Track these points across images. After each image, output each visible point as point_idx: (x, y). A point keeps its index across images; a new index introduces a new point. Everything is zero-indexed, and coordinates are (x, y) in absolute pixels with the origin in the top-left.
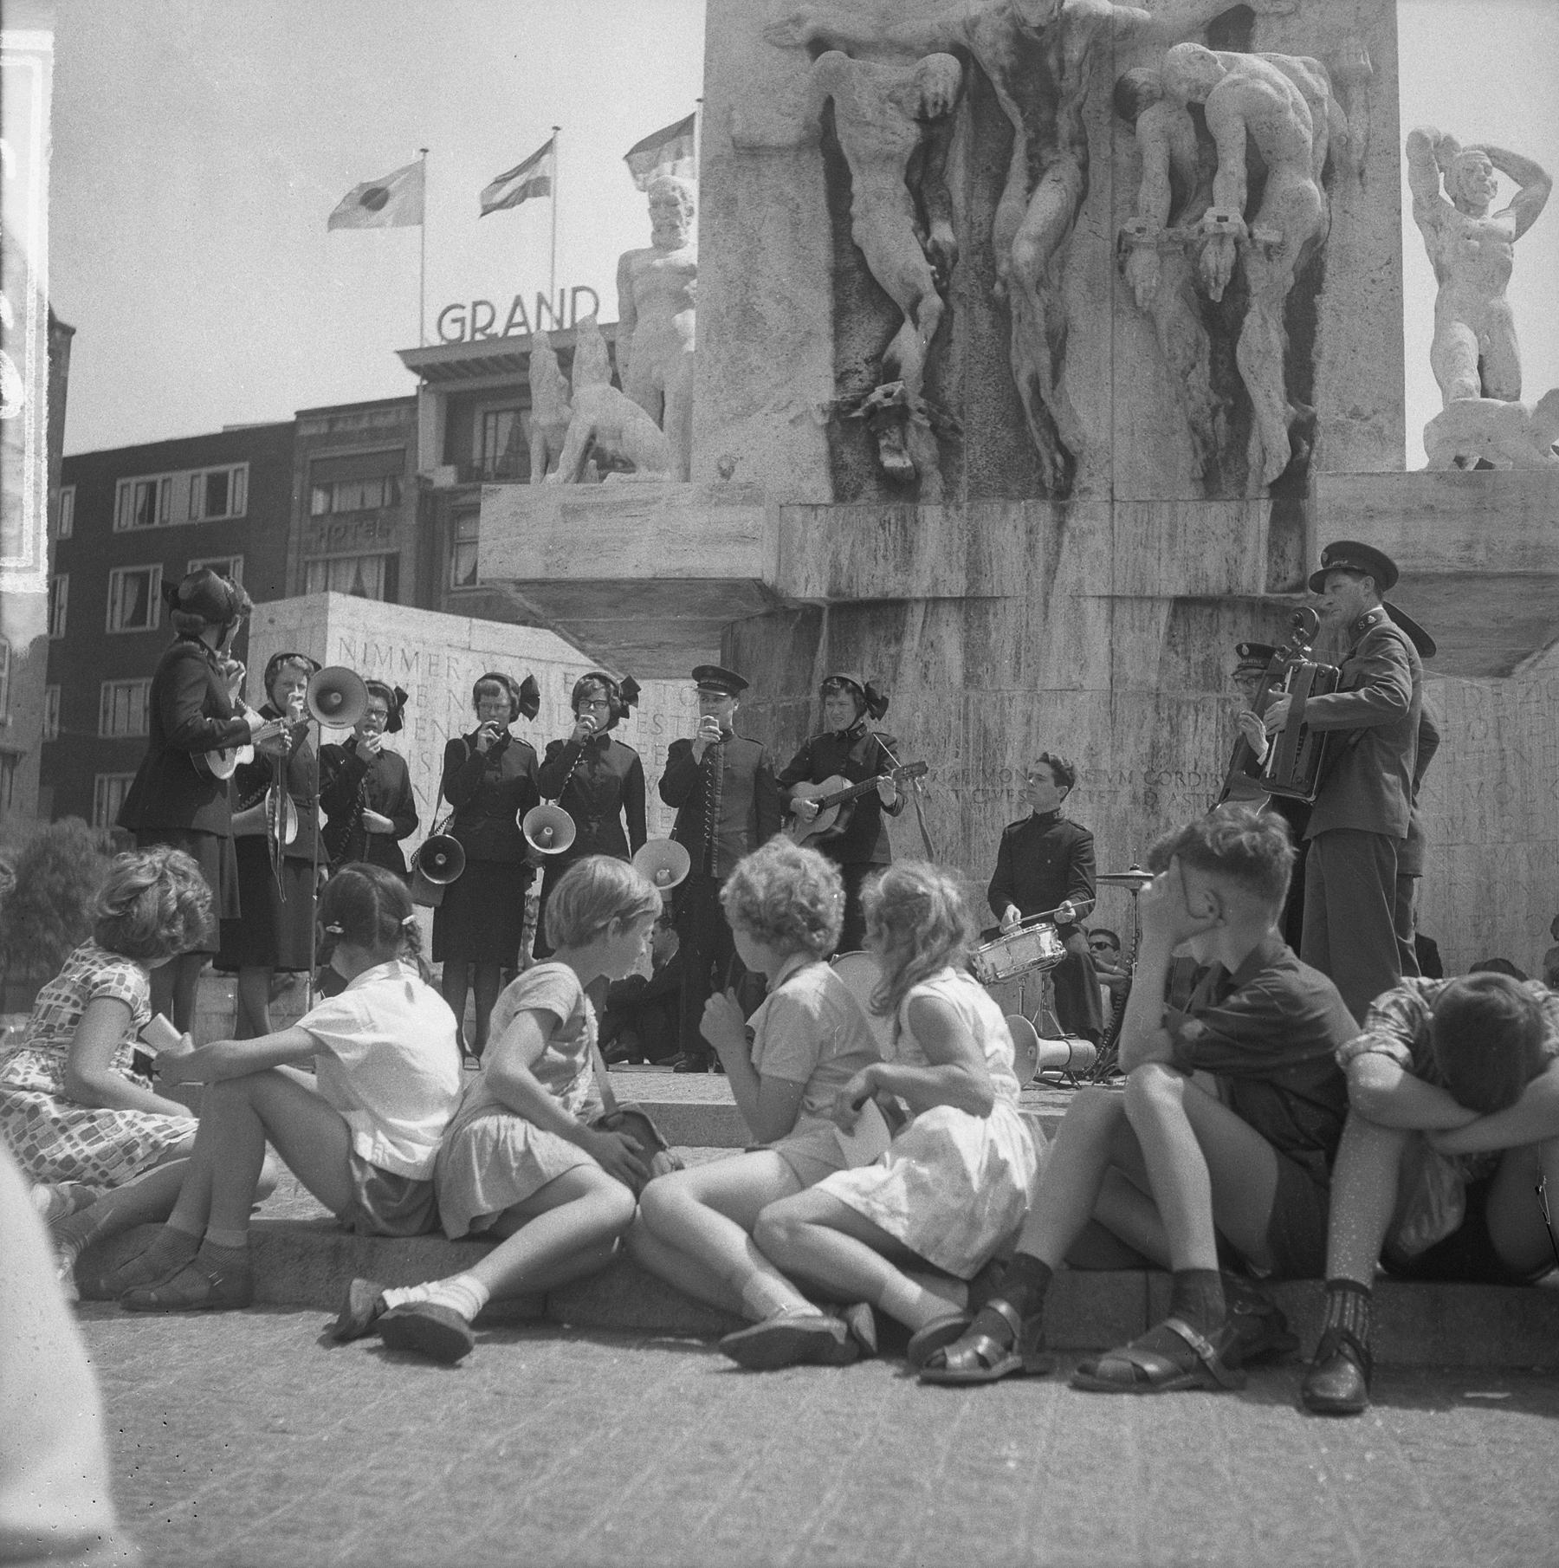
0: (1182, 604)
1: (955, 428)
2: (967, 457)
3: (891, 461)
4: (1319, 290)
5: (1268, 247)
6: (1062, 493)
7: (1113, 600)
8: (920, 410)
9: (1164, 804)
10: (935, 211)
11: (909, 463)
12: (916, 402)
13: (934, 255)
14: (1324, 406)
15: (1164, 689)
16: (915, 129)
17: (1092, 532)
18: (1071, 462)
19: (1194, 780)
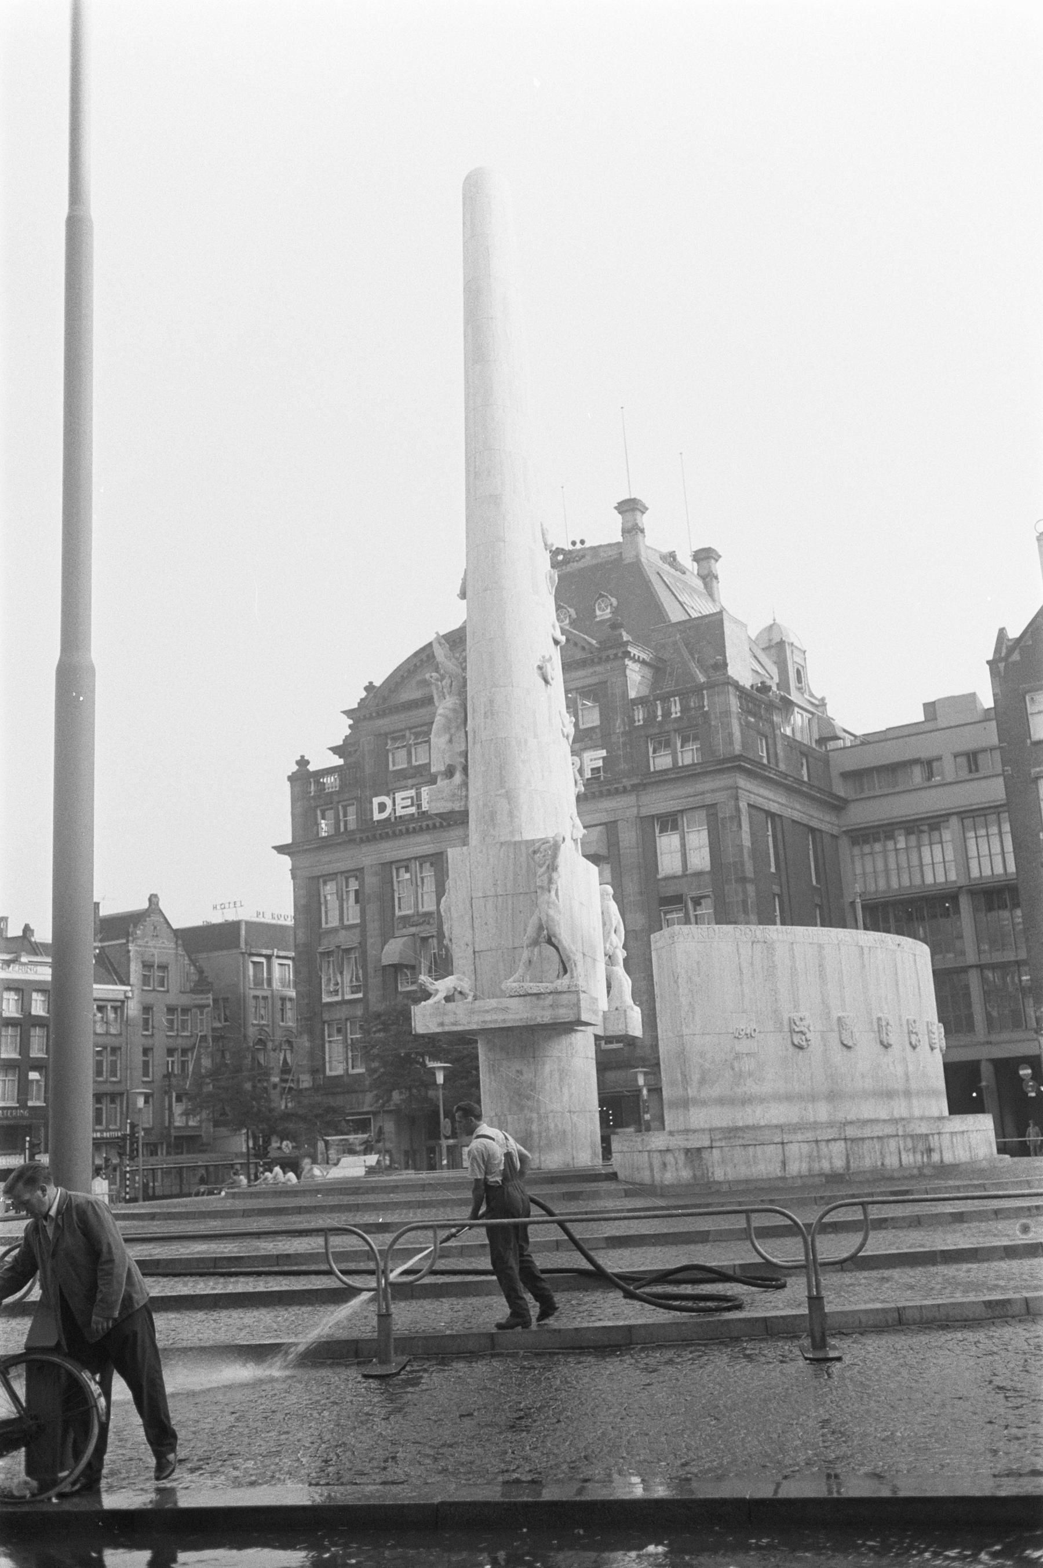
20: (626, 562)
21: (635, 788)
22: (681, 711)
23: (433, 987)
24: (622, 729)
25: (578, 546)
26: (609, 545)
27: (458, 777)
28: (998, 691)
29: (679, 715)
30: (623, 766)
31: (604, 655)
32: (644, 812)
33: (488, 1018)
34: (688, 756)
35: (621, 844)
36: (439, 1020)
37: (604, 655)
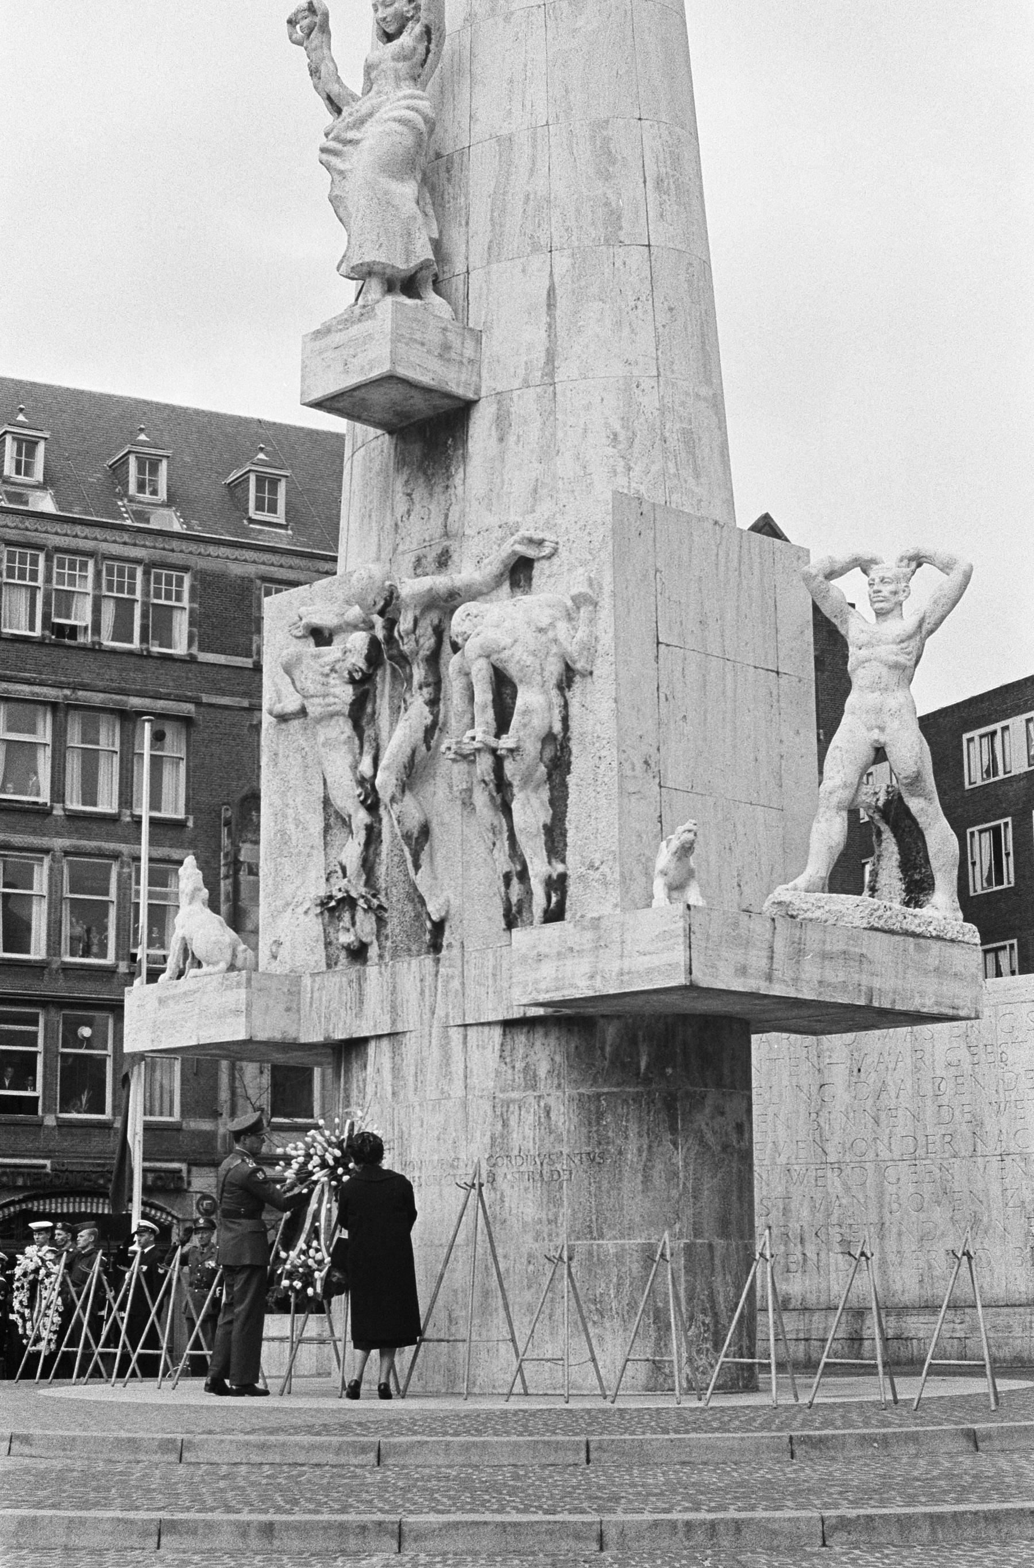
0: (509, 1025)
1: (380, 907)
2: (388, 930)
3: (346, 938)
4: (569, 772)
5: (511, 751)
6: (436, 947)
7: (466, 1026)
8: (363, 897)
9: (499, 1179)
10: (366, 748)
11: (353, 938)
12: (357, 890)
13: (361, 782)
14: (573, 864)
15: (498, 1094)
16: (350, 689)
17: (452, 977)
18: (439, 927)
19: (519, 1161)
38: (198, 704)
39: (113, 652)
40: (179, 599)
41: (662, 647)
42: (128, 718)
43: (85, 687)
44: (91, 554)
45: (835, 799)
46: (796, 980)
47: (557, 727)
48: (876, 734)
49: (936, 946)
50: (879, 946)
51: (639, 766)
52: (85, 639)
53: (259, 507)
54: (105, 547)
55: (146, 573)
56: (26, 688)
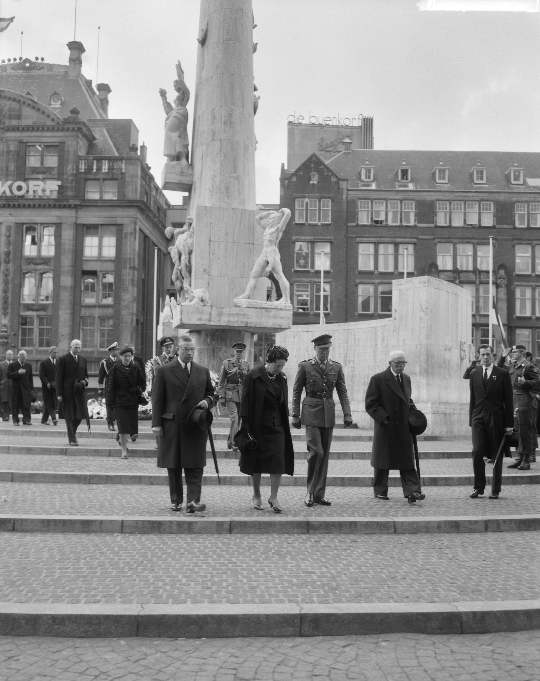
20: (70, 78)
21: (76, 207)
22: (109, 169)
23: (192, 295)
24: (71, 172)
25: (39, 61)
26: (60, 66)
27: (183, 161)
28: (283, 194)
29: (106, 171)
30: (70, 193)
31: (66, 126)
32: (81, 221)
33: (232, 319)
34: (110, 196)
35: (63, 237)
36: (199, 316)
37: (66, 126)
38: (417, 239)
39: (392, 227)
40: (412, 209)
41: (211, 242)
42: (397, 245)
43: (383, 237)
44: (385, 199)
45: (253, 276)
46: (219, 321)
47: (188, 263)
48: (265, 258)
49: (274, 311)
50: (251, 312)
51: (202, 270)
52: (384, 223)
53: (440, 179)
54: (388, 197)
55: (401, 203)
56: (366, 239)
